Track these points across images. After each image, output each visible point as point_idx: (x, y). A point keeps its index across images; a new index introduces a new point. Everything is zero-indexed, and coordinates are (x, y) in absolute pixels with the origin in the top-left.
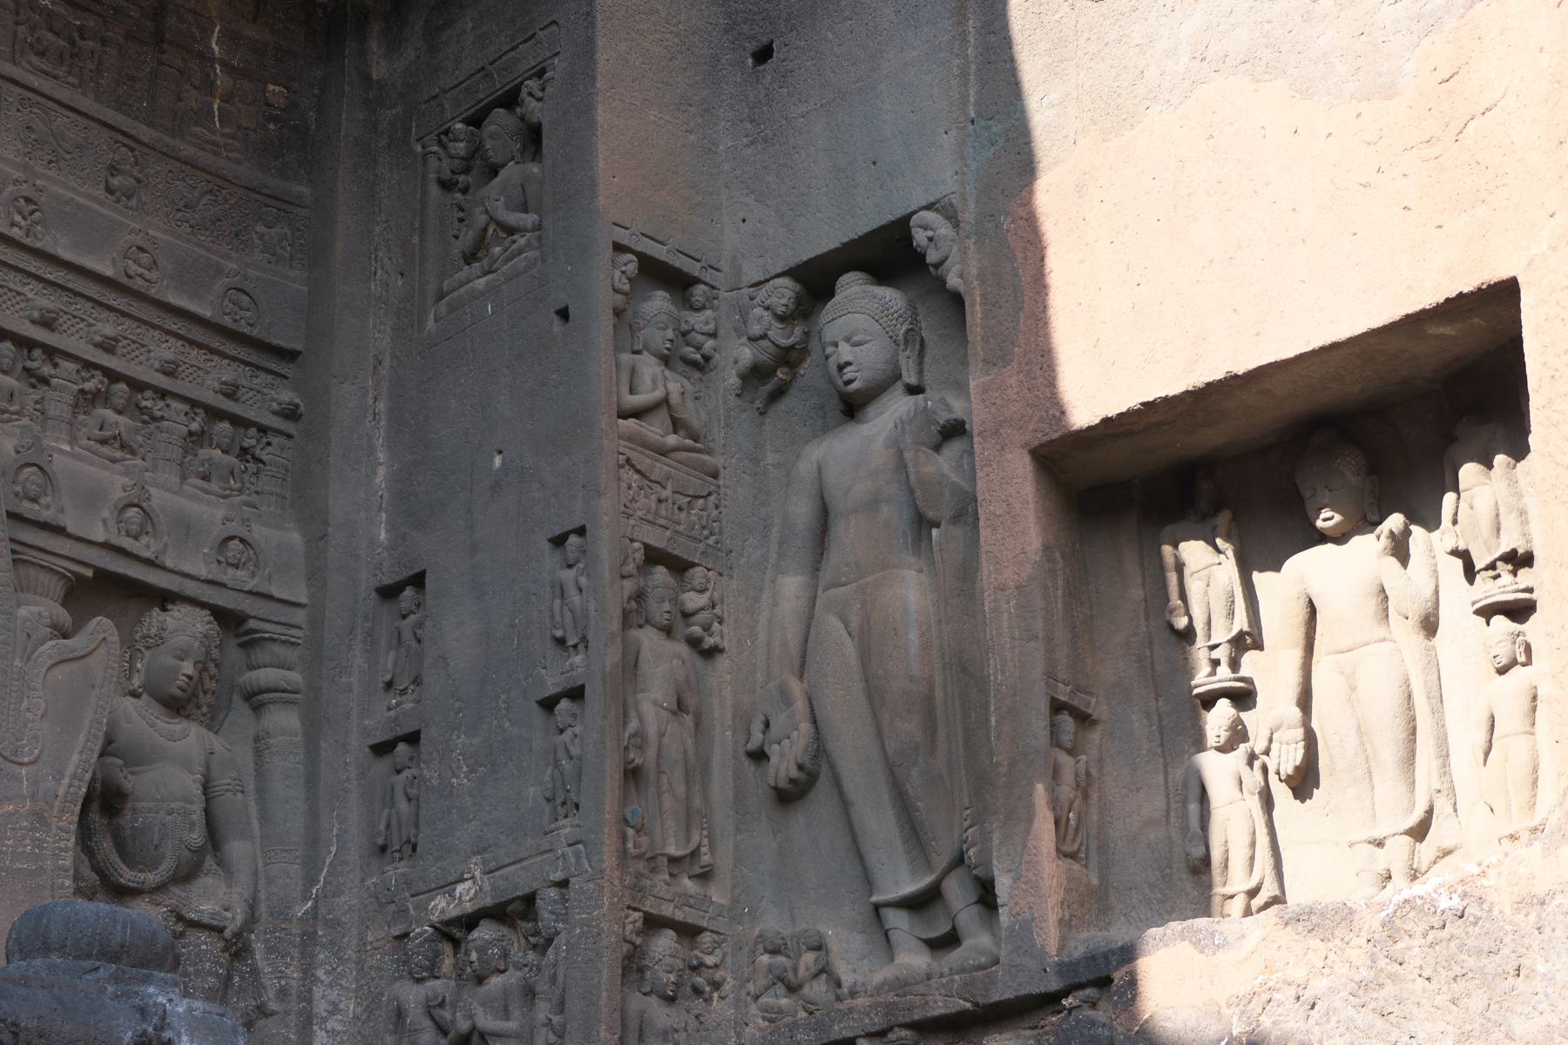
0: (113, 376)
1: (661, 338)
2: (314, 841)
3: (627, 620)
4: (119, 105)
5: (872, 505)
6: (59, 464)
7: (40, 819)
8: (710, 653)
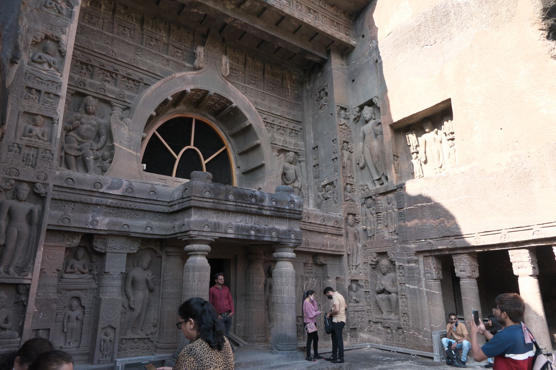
0: (281, 126)
1: (343, 116)
2: (308, 177)
3: (342, 149)
4: (279, 95)
5: (370, 133)
7: (277, 177)
8: (352, 152)
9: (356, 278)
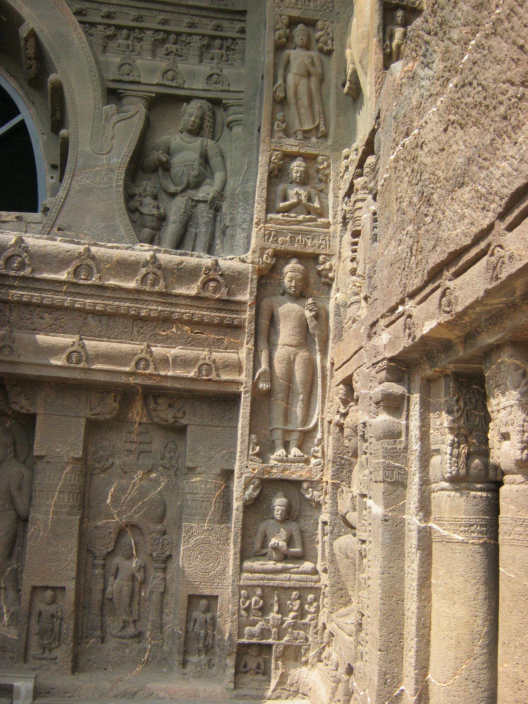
0: (168, 33)
6: (138, 62)
9: (286, 475)
